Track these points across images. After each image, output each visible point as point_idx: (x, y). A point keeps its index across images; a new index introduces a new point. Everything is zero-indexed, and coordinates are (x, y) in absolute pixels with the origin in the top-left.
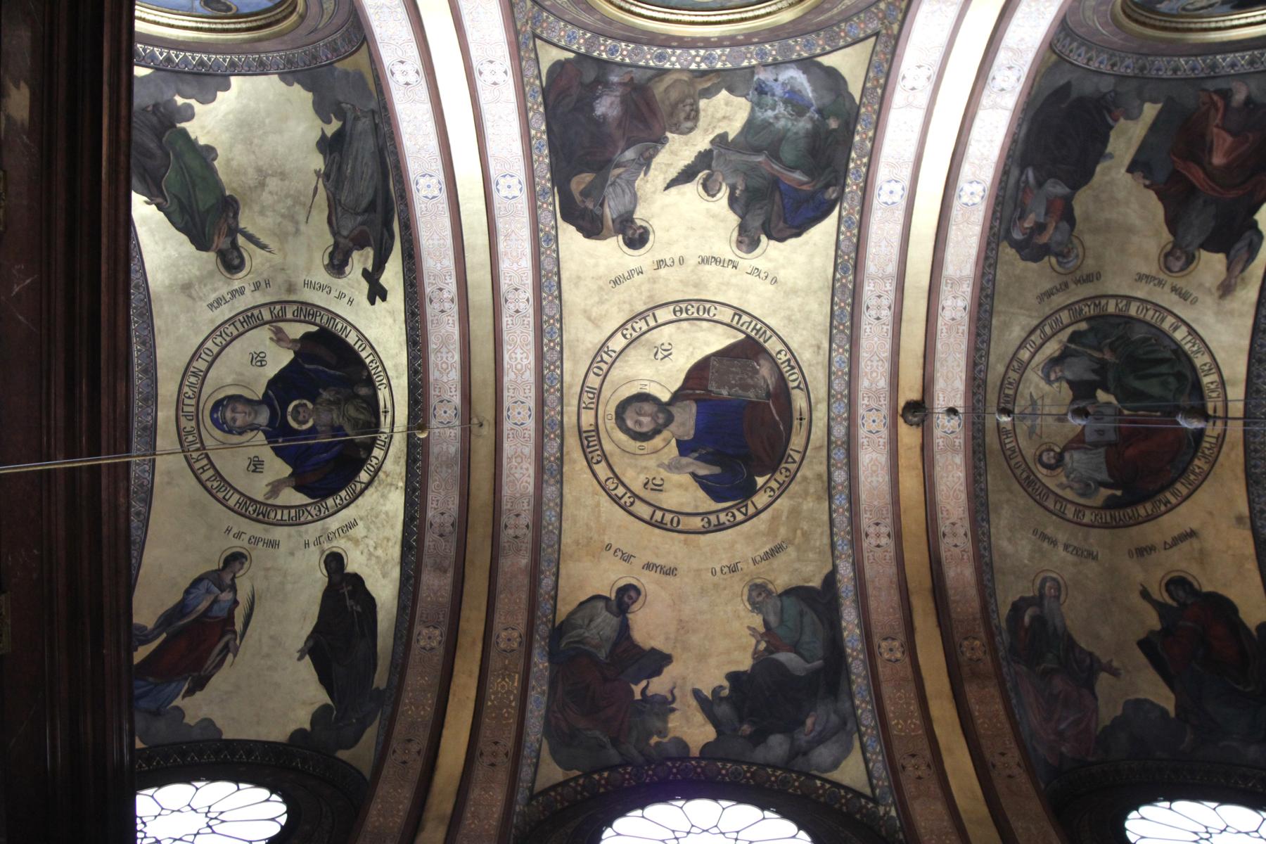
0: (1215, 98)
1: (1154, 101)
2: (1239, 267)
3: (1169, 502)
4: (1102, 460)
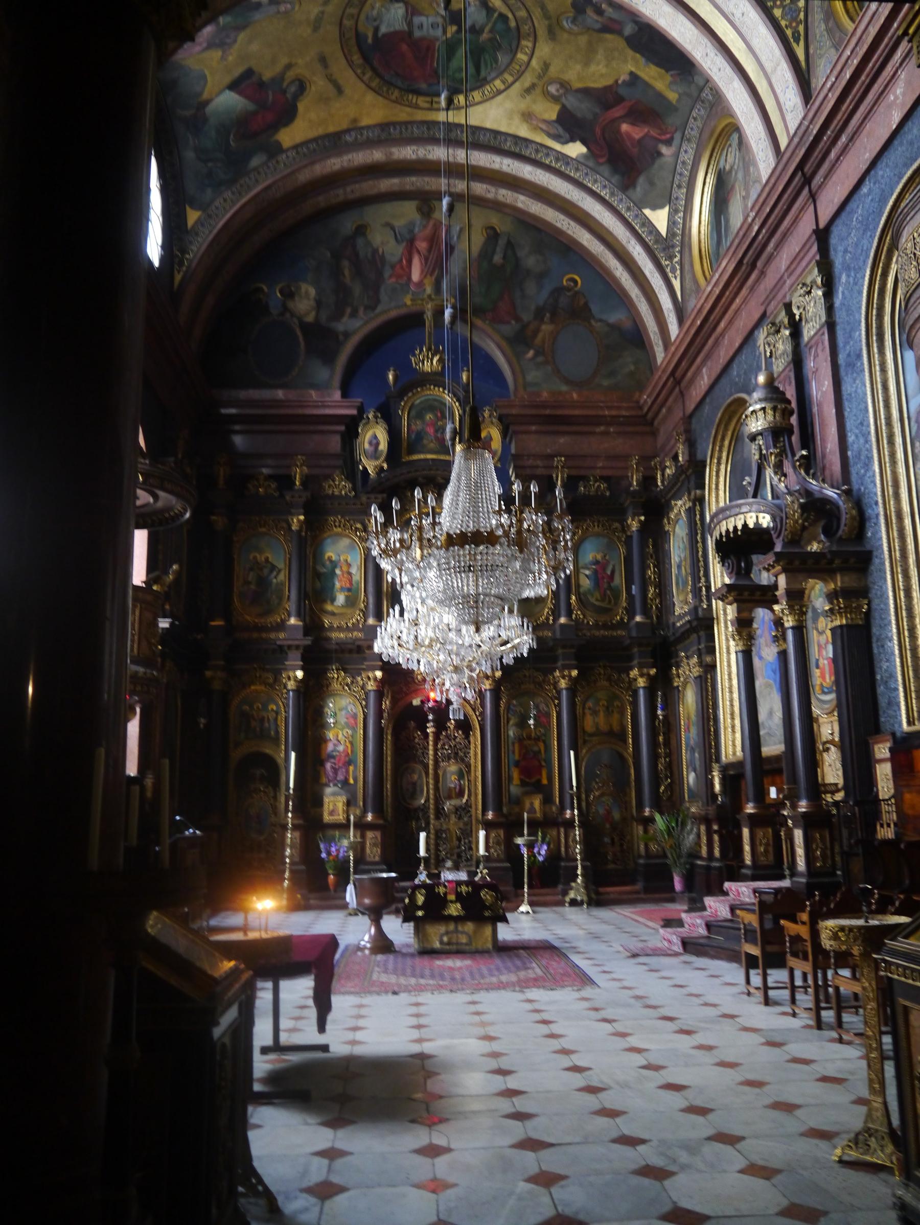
0: (668, 136)
1: (678, 101)
4: (397, 28)
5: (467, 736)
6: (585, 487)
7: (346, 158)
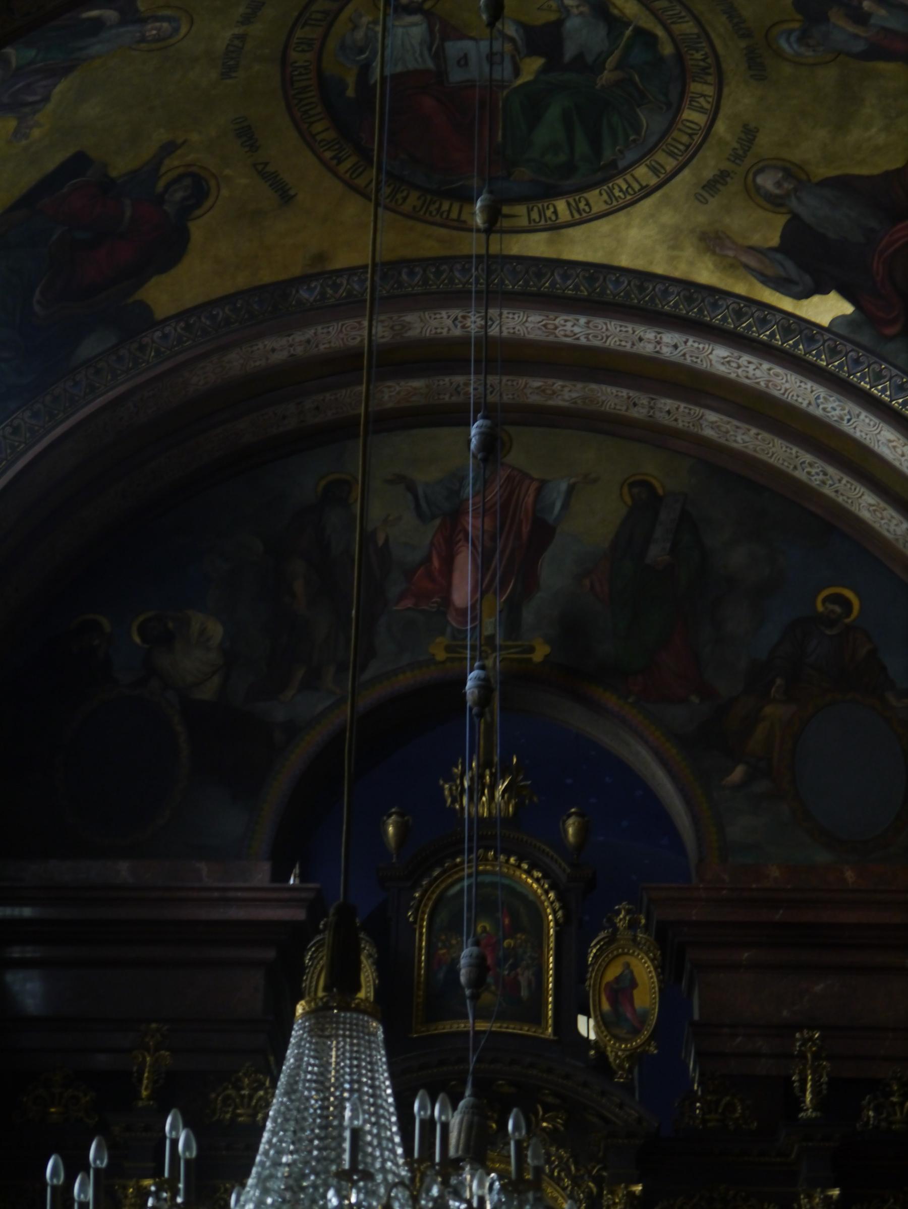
2: (753, 263)
3: (339, 163)
4: (412, 65)
6: (877, 1110)
7: (299, 337)
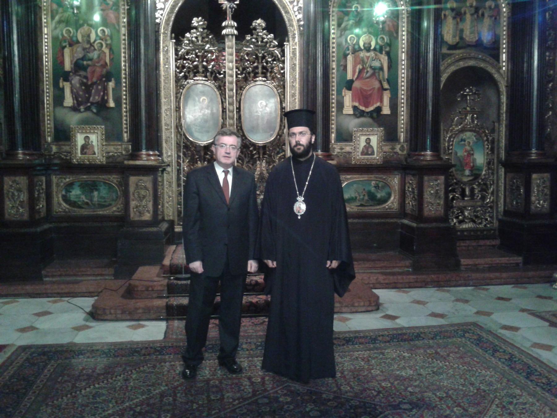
5: (281, 46)
